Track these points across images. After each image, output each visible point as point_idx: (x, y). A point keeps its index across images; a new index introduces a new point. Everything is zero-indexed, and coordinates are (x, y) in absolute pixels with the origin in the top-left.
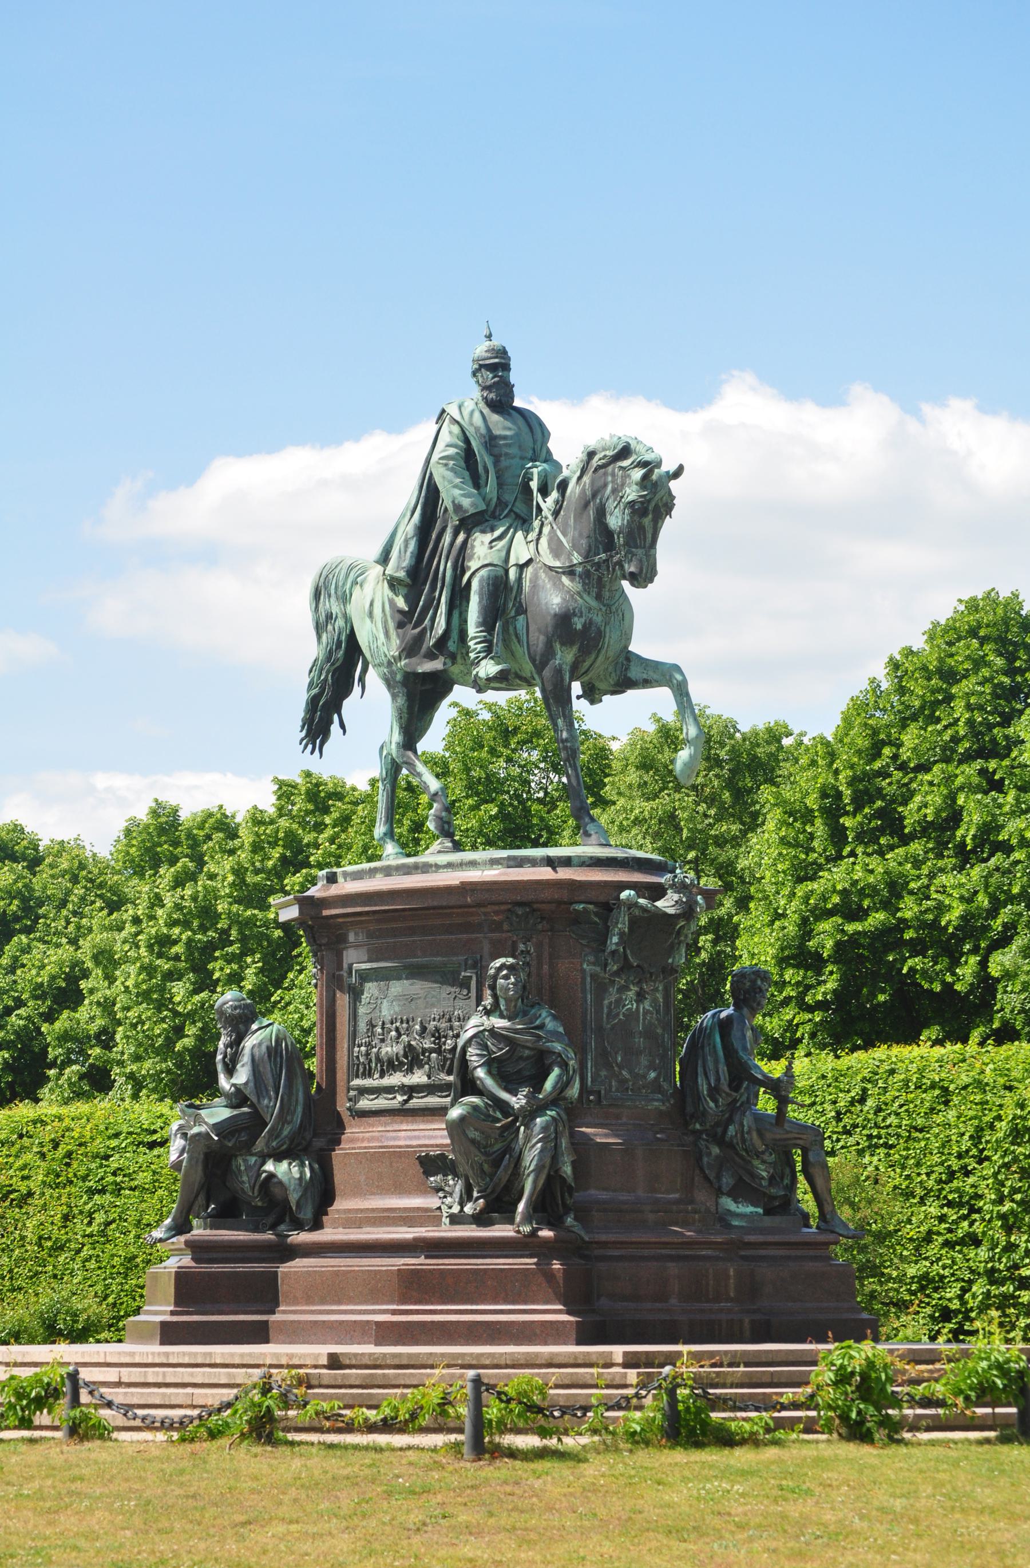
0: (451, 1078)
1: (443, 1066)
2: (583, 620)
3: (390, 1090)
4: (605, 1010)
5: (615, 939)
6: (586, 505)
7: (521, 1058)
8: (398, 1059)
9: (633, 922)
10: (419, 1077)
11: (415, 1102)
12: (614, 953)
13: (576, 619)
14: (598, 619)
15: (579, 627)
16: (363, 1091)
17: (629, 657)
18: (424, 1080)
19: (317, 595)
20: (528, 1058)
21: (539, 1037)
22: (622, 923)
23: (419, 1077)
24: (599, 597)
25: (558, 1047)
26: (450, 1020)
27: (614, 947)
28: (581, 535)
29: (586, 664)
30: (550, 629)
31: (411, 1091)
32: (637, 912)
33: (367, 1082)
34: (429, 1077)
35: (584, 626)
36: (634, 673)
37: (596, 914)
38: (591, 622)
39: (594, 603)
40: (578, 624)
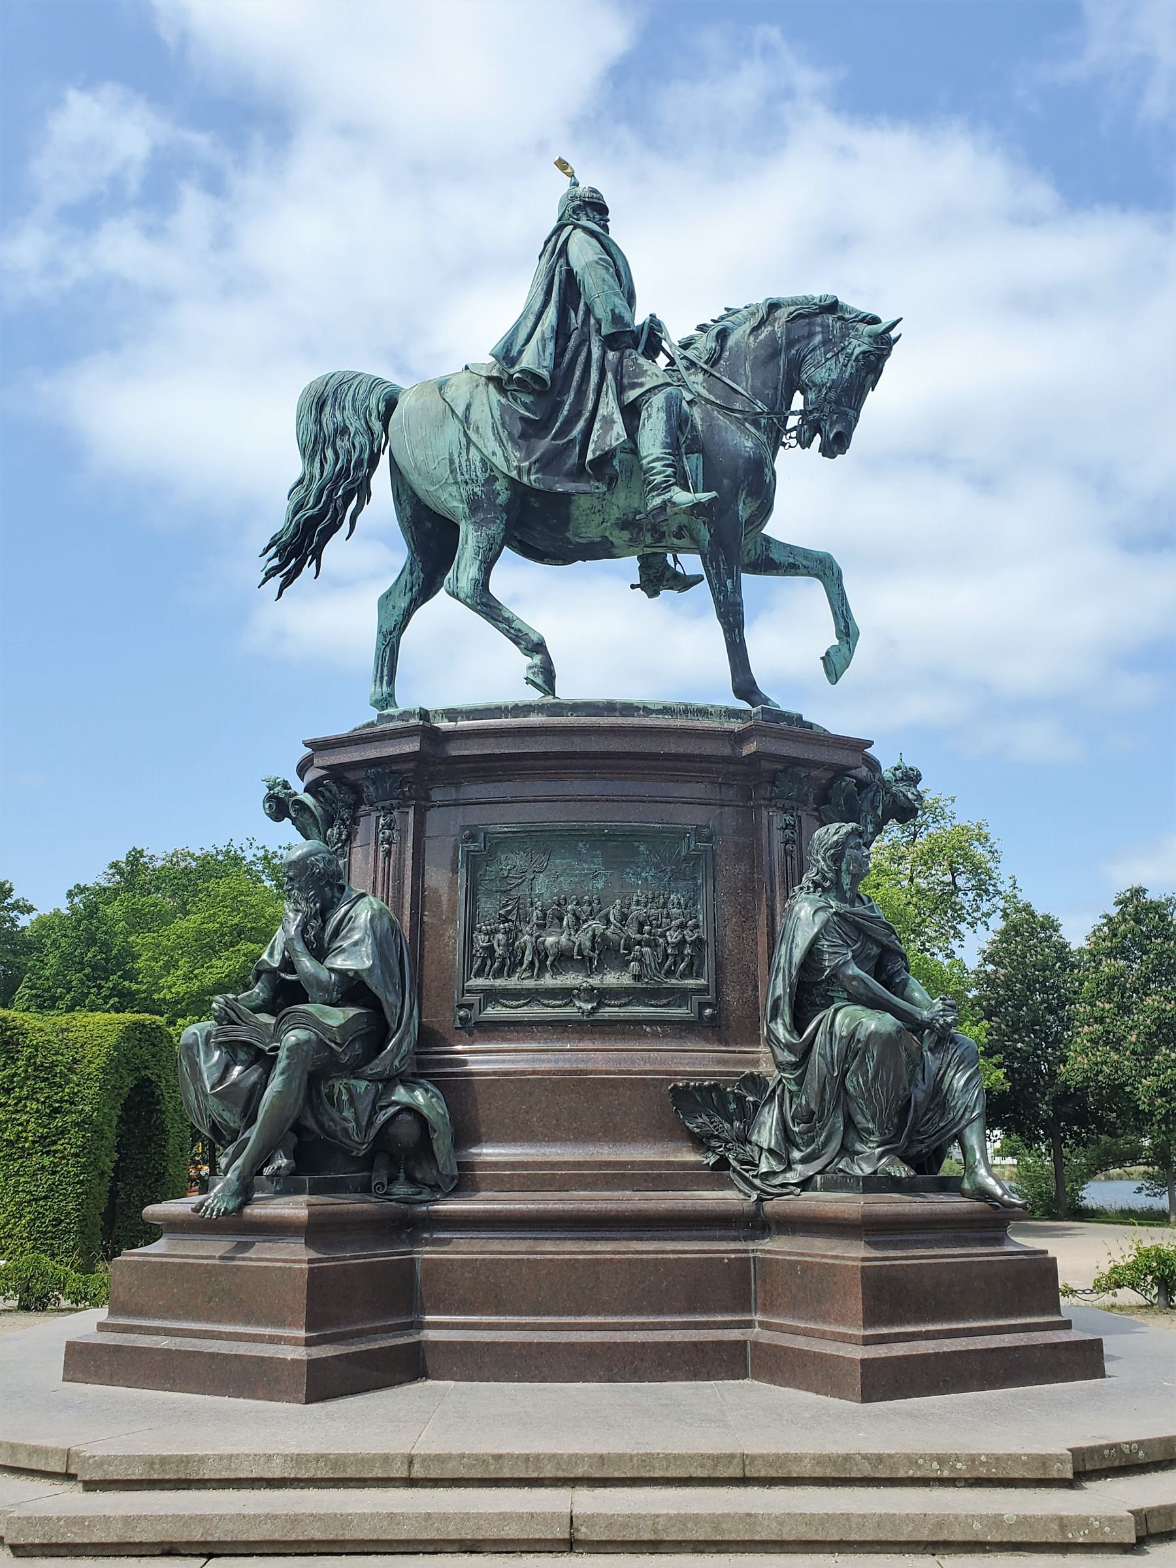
0: (702, 981)
1: (661, 965)
3: (567, 994)
6: (775, 354)
8: (580, 952)
10: (612, 979)
11: (607, 1012)
16: (492, 996)
18: (626, 980)
23: (612, 979)
26: (664, 905)
28: (764, 384)
30: (740, 473)
31: (601, 996)
33: (513, 982)
34: (637, 978)
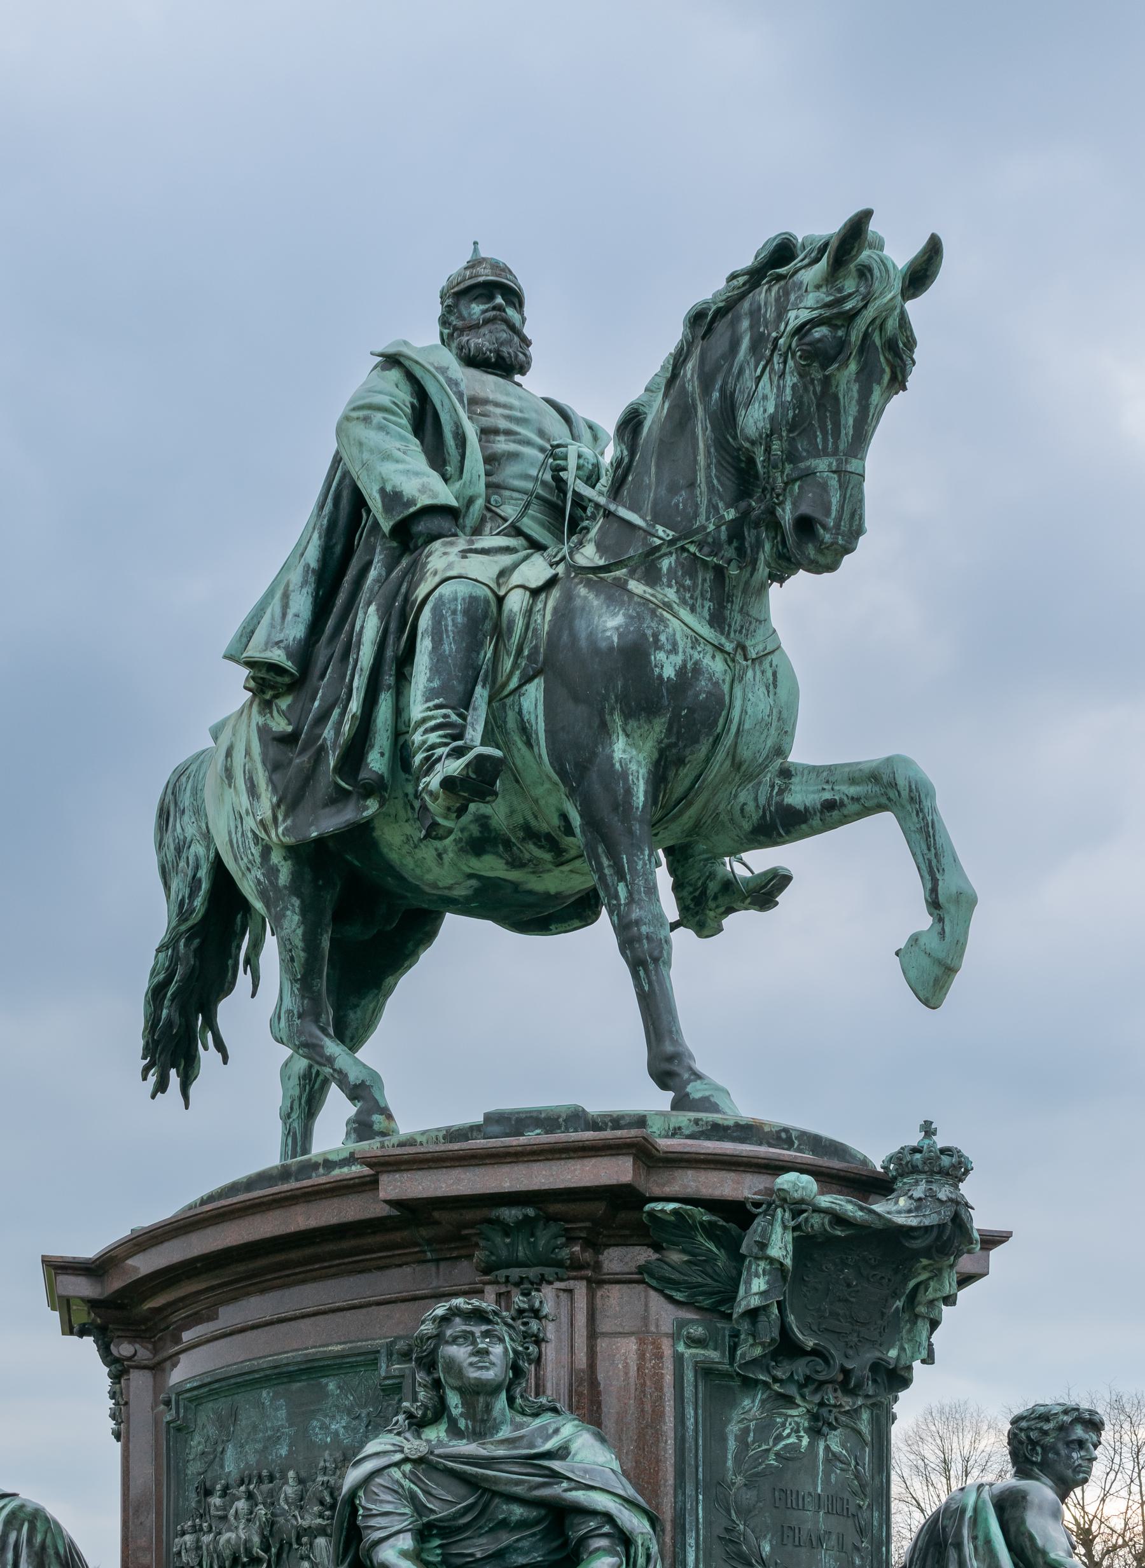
2: (678, 659)
4: (732, 1444)
5: (759, 1284)
7: (504, 1524)
9: (805, 1245)
12: (753, 1314)
13: (661, 656)
14: (716, 666)
15: (669, 672)
17: (786, 773)
19: (164, 816)
20: (523, 1524)
21: (556, 1476)
22: (780, 1246)
24: (717, 620)
25: (601, 1501)
27: (755, 1302)
29: (686, 775)
32: (817, 1221)
35: (681, 672)
36: (799, 796)
37: (710, 1230)
38: (697, 669)
39: (706, 631)
40: (667, 666)
